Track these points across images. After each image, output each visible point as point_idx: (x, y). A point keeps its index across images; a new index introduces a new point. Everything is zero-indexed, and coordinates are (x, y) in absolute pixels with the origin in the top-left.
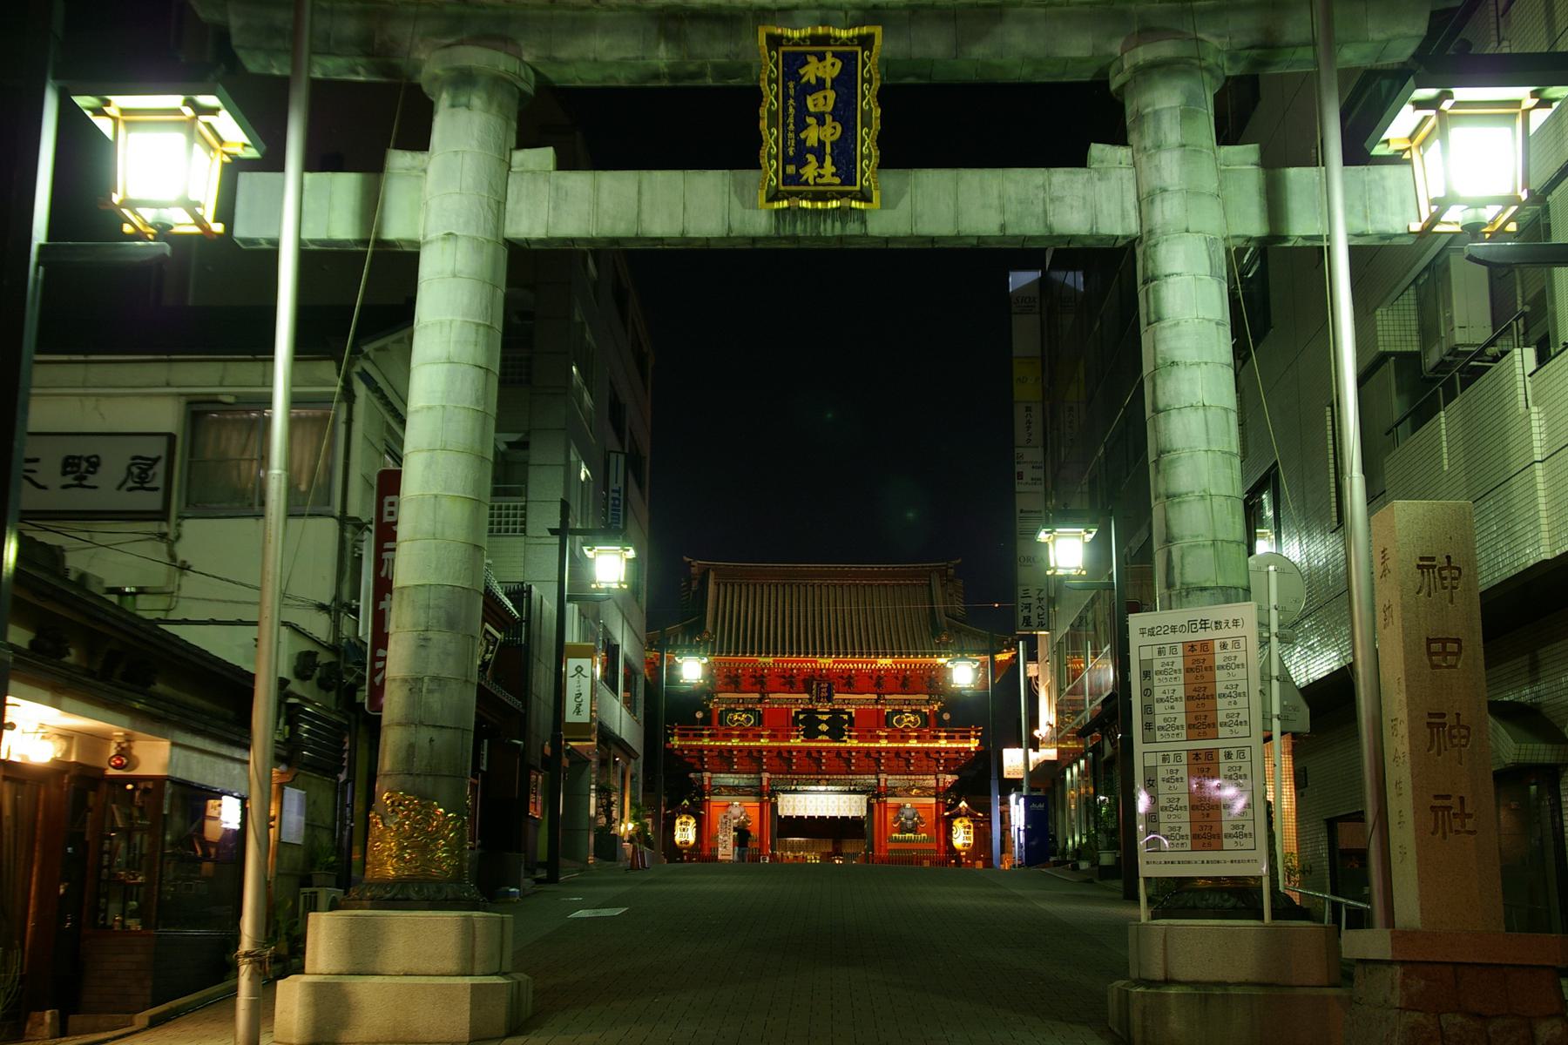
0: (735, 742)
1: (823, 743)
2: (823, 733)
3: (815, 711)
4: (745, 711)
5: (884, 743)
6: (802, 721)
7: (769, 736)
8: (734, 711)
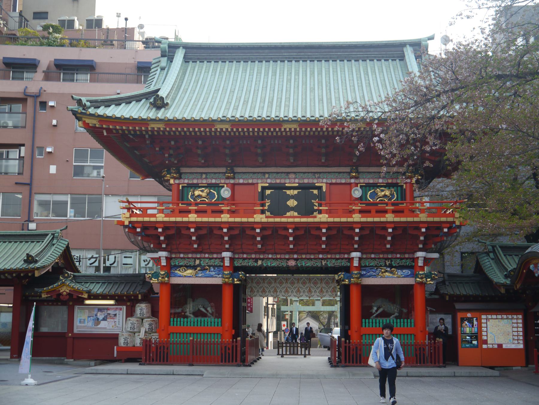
0: (193, 217)
1: (292, 217)
3: (281, 187)
4: (210, 186)
5: (357, 218)
7: (232, 212)
8: (196, 186)
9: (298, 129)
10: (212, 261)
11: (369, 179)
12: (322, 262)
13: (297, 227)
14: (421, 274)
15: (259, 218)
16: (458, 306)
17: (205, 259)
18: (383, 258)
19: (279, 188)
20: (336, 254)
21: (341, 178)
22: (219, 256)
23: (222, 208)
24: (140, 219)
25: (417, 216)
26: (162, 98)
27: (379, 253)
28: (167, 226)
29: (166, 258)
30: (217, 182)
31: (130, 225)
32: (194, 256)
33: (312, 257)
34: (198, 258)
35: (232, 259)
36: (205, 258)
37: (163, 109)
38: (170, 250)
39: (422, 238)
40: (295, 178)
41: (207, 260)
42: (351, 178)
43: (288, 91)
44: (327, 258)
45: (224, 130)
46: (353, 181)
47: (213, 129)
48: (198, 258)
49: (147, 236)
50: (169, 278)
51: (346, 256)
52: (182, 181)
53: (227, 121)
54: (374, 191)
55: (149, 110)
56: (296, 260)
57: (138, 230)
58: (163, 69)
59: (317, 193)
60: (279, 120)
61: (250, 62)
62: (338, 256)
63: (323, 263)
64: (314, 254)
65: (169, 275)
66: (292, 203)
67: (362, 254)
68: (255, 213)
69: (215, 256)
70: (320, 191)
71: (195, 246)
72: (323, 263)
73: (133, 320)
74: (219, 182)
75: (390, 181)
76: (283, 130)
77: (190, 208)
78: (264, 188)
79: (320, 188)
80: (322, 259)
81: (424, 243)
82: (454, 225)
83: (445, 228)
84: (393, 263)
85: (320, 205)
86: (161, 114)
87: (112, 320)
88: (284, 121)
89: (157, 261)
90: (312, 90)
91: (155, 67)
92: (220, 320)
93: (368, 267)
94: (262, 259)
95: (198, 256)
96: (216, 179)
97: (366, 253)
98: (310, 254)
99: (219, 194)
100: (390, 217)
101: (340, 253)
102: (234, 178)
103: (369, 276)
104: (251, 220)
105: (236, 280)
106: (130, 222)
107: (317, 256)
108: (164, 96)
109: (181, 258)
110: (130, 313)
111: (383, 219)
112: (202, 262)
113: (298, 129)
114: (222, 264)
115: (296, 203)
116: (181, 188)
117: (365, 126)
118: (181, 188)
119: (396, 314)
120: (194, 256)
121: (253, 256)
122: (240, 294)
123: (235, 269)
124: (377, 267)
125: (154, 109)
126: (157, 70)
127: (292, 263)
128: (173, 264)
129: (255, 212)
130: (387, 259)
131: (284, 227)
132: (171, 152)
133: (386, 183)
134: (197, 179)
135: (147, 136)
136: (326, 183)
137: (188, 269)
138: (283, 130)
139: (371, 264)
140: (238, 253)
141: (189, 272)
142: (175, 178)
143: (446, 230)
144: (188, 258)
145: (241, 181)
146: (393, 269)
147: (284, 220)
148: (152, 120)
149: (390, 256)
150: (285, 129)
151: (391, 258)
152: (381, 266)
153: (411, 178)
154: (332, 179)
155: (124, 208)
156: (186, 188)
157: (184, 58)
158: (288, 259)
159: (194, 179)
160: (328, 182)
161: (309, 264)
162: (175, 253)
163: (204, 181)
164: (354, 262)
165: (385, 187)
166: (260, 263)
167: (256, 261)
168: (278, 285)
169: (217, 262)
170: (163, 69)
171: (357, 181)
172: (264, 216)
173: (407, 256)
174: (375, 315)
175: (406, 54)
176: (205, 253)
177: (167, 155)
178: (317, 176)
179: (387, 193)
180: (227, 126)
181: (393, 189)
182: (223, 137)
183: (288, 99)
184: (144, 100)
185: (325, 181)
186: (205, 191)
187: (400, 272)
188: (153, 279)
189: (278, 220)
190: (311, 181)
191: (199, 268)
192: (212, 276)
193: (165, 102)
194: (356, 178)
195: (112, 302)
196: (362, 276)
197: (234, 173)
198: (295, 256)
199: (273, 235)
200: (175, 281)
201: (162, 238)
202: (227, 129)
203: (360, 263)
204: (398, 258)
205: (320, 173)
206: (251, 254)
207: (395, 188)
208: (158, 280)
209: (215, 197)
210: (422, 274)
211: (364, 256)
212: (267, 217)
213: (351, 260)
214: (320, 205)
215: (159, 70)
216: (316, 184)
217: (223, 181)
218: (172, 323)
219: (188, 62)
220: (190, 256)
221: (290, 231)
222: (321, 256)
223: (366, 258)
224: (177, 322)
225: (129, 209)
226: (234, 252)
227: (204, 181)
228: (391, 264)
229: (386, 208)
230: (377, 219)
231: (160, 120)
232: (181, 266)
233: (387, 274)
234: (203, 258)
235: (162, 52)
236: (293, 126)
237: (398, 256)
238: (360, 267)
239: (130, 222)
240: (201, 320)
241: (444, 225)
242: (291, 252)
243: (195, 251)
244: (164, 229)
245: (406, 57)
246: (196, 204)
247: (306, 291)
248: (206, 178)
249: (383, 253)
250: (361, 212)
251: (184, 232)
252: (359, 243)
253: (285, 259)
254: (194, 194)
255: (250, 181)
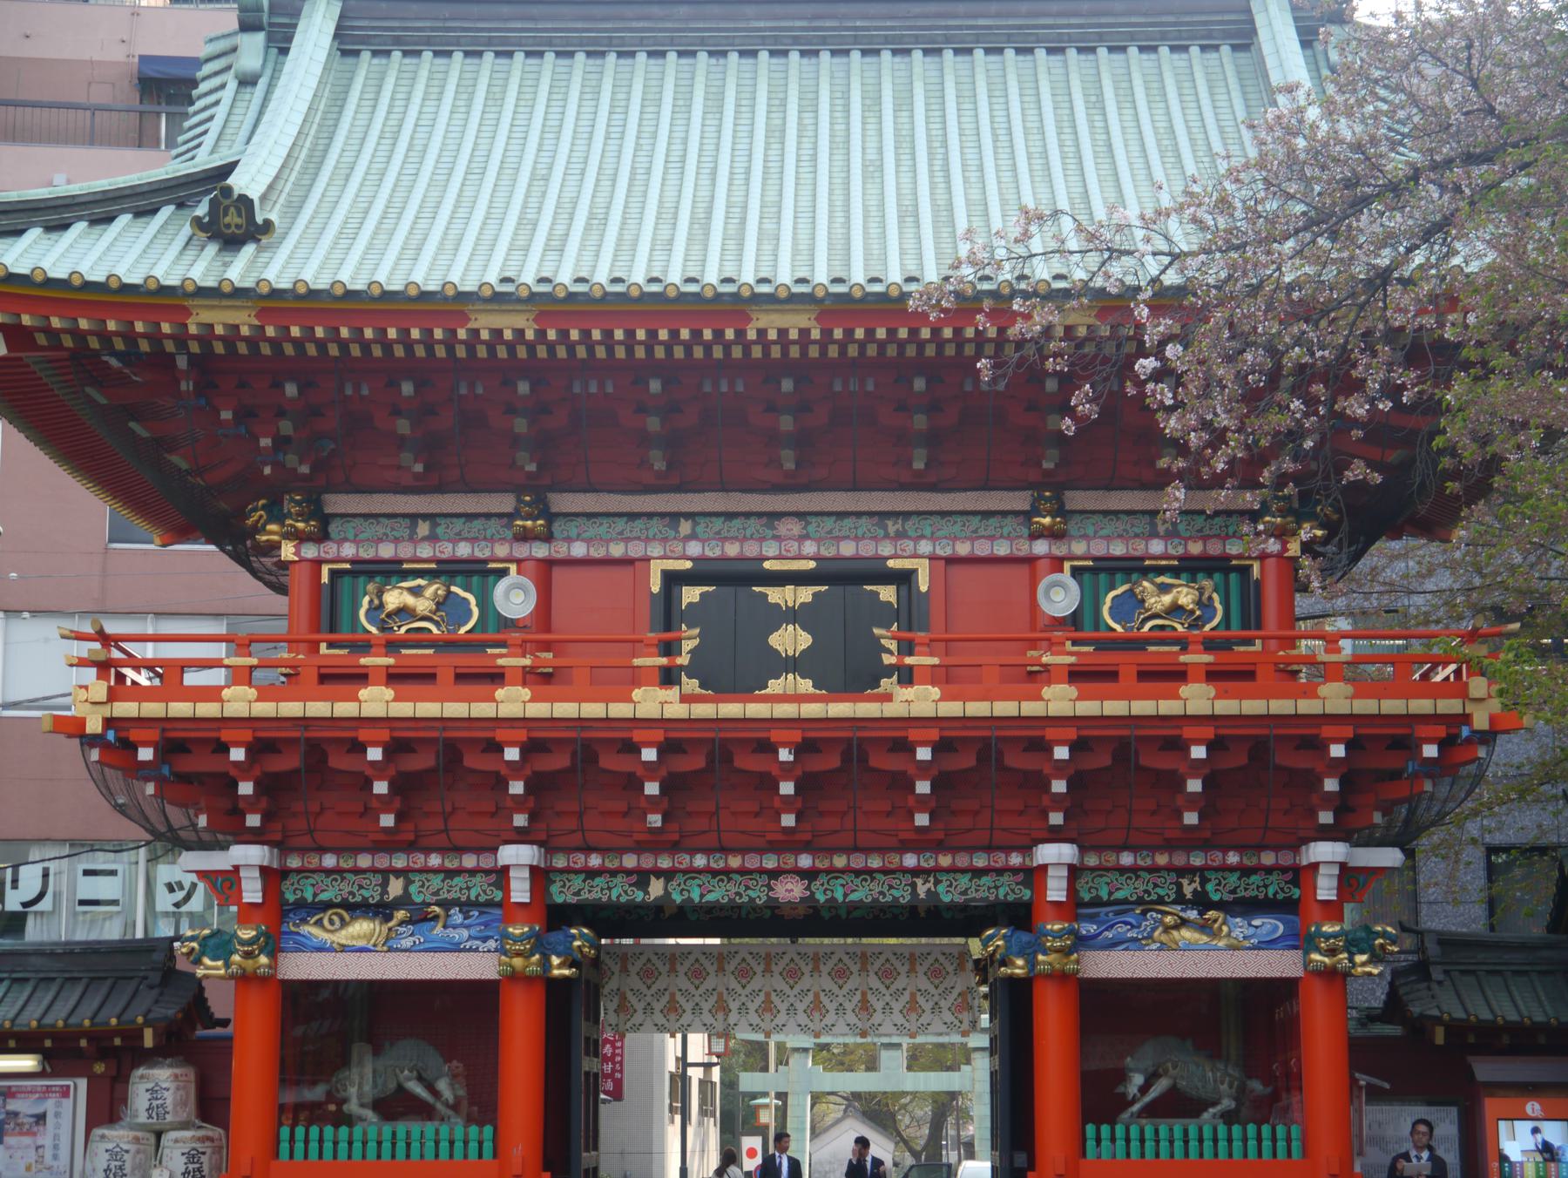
0: (376, 701)
1: (790, 699)
2: (793, 665)
4: (447, 570)
5: (1059, 700)
6: (695, 614)
8: (391, 571)
9: (816, 334)
10: (458, 881)
11: (1108, 538)
12: (914, 886)
13: (812, 739)
14: (1328, 937)
15: (652, 702)
16: (1485, 1069)
17: (425, 874)
18: (1169, 868)
19: (739, 578)
20: (972, 849)
21: (992, 538)
22: (486, 862)
23: (500, 662)
24: (153, 709)
25: (1310, 692)
26: (245, 203)
27: (1154, 849)
28: (266, 739)
29: (264, 870)
30: (479, 554)
31: (111, 735)
32: (382, 861)
33: (875, 862)
34: (398, 873)
35: (539, 876)
36: (426, 870)
37: (249, 249)
38: (278, 837)
39: (1331, 785)
40: (802, 538)
41: (436, 881)
42: (1034, 537)
43: (772, 174)
44: (937, 870)
45: (508, 335)
46: (1041, 547)
47: (462, 334)
48: (398, 873)
49: (184, 779)
50: (273, 955)
51: (1015, 860)
52: (330, 549)
53: (519, 300)
54: (1131, 590)
55: (191, 253)
56: (809, 875)
57: (146, 754)
58: (247, 81)
59: (893, 599)
60: (736, 296)
61: (612, 58)
62: (980, 861)
63: (922, 890)
64: (882, 850)
65: (273, 944)
66: (790, 640)
67: (1083, 850)
68: (636, 683)
69: (469, 861)
70: (904, 589)
71: (387, 820)
72: (922, 890)
73: (117, 1136)
74: (487, 554)
75: (1195, 548)
76: (752, 335)
77: (363, 661)
78: (673, 580)
79: (904, 579)
80: (917, 872)
81: (1341, 804)
82: (1465, 732)
83: (1429, 741)
84: (1210, 887)
85: (907, 648)
86: (241, 269)
87: (27, 1140)
88: (756, 298)
89: (225, 883)
90: (873, 170)
91: (216, 74)
92: (488, 1130)
93: (1108, 903)
94: (668, 875)
95: (400, 862)
96: (473, 540)
97: (1099, 849)
98: (867, 851)
99: (485, 602)
100: (1197, 698)
101: (989, 849)
102: (548, 538)
103: (1113, 945)
104: (619, 710)
105: (555, 960)
106: (109, 722)
107: (894, 860)
108: (254, 194)
109: (328, 872)
110: (106, 1108)
111: (1168, 707)
112: (413, 889)
113: (816, 334)
114: (498, 895)
115: (805, 640)
116: (325, 579)
117: (1092, 321)
118: (325, 579)
119: (1227, 1104)
120: (382, 861)
121: (630, 861)
122: (572, 1022)
123: (557, 917)
124: (1145, 904)
125: (212, 249)
126: (223, 86)
127: (790, 890)
128: (291, 897)
129: (637, 678)
130: (1187, 871)
131: (759, 737)
132: (286, 427)
133: (1180, 558)
134: (396, 541)
135: (182, 362)
136: (933, 558)
137: (353, 919)
138: (752, 335)
139: (1119, 895)
140: (568, 850)
141: (362, 928)
142: (300, 538)
143: (1430, 751)
144: (357, 871)
145: (579, 550)
146: (1211, 914)
147: (756, 710)
148: (202, 292)
149: (1197, 860)
150: (762, 333)
151: (1201, 870)
152: (1161, 901)
153: (1282, 534)
154: (955, 539)
155: (82, 663)
156: (347, 580)
157: (336, 36)
158: (775, 874)
159: (380, 540)
160: (940, 552)
161: (862, 893)
162: (302, 851)
163: (425, 551)
164: (1051, 883)
165: (1175, 572)
166: (656, 888)
167: (643, 884)
168: (734, 984)
169: (479, 888)
170: (247, 81)
171: (1059, 549)
172: (673, 693)
173: (1268, 859)
174: (1136, 1108)
175: (1260, 20)
176: (427, 851)
177: (265, 442)
178: (892, 527)
179: (1185, 596)
180: (520, 321)
181: (1208, 584)
182: (500, 365)
183: (772, 210)
184: (167, 211)
185: (925, 547)
186: (429, 592)
187: (1239, 928)
188: (207, 961)
189: (731, 710)
190: (867, 549)
191: (400, 914)
192: (456, 948)
193: (259, 219)
194: (1055, 535)
195: (27, 1063)
196: (1082, 942)
197: (551, 517)
198: (805, 861)
199: (712, 771)
200: (299, 967)
201: (246, 788)
202: (520, 333)
203: (1072, 890)
204: (1232, 869)
205: (906, 515)
206: (622, 851)
207: (1217, 576)
208: (227, 965)
209: (474, 616)
210: (1335, 936)
211: (1092, 860)
212: (684, 699)
213: (1035, 876)
214: (907, 648)
215: (232, 85)
216: (891, 563)
217: (502, 550)
218: (284, 1147)
219: (356, 53)
220: (364, 861)
221: (785, 755)
222: (910, 860)
223: (1100, 869)
224: (307, 1142)
225: (103, 667)
226: (547, 846)
227: (425, 551)
228: (1205, 893)
229: (1183, 658)
230: (1143, 707)
231: (239, 293)
232: (328, 905)
233: (1186, 934)
234: (420, 871)
235: (242, 10)
236: (796, 321)
237: (1233, 858)
238: (1073, 907)
239: (109, 722)
240: (408, 1133)
241: (1422, 731)
242: (788, 843)
243: (387, 843)
244: (257, 749)
245: (1263, 34)
246: (392, 646)
247: (849, 1006)
248: (433, 538)
249: (1169, 846)
250: (1075, 675)
251: (339, 761)
252: (1072, 804)
253: (762, 871)
254: (381, 606)
255: (617, 551)
